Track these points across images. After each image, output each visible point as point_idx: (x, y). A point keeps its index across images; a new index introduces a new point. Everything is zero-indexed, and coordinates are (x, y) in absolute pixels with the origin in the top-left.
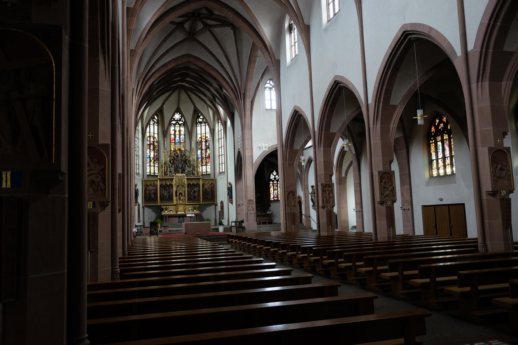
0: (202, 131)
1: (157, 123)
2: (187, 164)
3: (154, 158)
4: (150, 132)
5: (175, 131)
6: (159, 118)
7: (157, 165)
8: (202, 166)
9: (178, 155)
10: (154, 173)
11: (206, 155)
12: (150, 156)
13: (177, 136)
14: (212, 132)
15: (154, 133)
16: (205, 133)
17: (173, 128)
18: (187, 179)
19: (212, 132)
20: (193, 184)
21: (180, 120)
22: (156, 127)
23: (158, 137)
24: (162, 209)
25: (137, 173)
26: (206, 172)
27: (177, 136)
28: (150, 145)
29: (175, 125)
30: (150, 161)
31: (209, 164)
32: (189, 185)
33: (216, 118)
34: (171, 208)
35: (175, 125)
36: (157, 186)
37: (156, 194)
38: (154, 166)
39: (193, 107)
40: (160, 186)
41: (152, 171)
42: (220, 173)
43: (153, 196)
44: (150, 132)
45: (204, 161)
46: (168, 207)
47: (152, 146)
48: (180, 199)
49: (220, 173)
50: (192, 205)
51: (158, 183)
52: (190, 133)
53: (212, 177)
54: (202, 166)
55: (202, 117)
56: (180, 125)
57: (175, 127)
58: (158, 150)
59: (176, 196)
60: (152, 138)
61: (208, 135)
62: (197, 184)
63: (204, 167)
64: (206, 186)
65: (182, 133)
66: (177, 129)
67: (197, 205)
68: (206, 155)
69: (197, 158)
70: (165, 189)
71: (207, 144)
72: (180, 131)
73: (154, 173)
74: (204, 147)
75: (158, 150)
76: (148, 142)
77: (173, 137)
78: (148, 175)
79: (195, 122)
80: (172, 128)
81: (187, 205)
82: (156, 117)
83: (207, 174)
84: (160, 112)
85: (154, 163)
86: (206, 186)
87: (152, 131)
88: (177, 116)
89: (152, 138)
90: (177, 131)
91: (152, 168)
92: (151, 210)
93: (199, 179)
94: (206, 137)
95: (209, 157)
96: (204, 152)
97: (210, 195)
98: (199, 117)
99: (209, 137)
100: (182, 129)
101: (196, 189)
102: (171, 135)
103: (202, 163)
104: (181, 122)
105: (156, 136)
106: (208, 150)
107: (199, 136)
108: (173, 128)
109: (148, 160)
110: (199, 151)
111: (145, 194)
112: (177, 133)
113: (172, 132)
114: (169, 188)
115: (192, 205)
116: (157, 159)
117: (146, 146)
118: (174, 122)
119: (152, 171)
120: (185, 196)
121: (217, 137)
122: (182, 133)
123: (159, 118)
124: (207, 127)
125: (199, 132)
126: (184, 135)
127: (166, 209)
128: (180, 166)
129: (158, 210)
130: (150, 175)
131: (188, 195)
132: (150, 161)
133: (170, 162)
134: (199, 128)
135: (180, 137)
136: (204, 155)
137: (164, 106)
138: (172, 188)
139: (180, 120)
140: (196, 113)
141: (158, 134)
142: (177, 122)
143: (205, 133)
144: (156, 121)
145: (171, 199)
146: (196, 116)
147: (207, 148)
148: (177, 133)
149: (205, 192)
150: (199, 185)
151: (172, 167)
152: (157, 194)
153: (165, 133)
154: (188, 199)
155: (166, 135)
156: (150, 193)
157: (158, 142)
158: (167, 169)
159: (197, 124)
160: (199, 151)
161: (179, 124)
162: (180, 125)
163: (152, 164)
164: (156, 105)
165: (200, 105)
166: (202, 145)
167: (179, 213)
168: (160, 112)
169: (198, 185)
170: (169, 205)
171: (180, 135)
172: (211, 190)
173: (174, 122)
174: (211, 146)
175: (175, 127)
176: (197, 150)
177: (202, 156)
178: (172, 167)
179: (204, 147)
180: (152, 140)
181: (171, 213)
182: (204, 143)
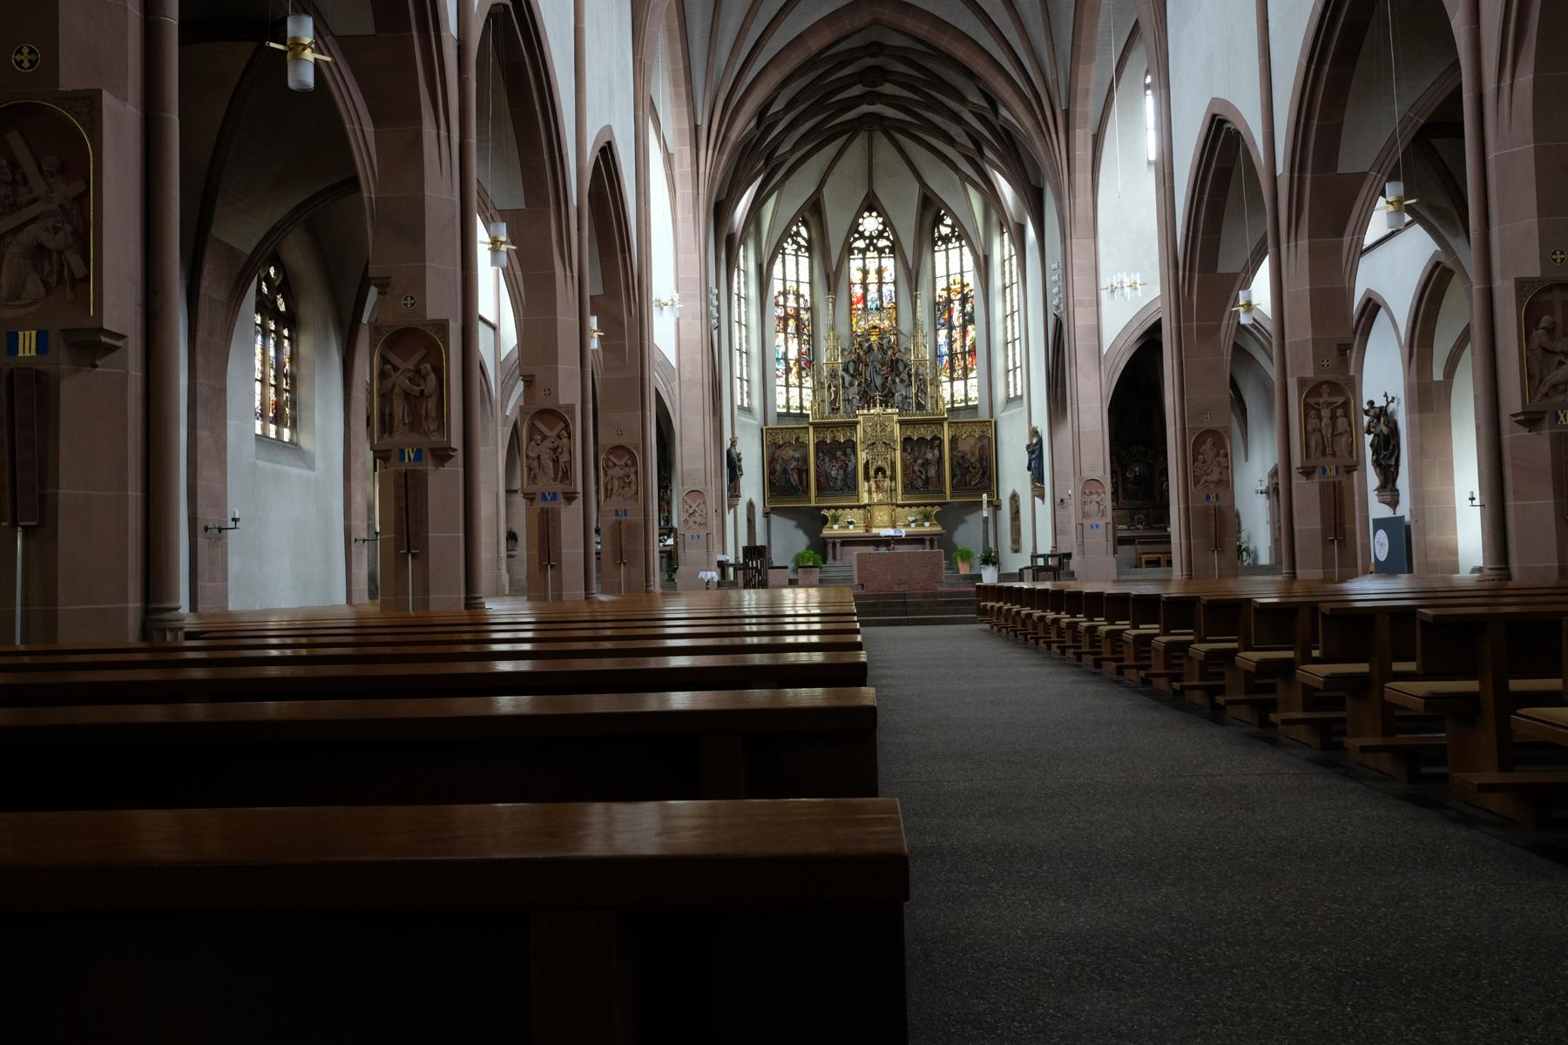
0: (951, 265)
1: (808, 249)
2: (898, 375)
3: (798, 361)
4: (784, 280)
5: (865, 272)
6: (814, 235)
7: (808, 382)
8: (952, 380)
9: (870, 347)
10: (801, 407)
11: (964, 346)
12: (785, 354)
13: (873, 288)
14: (983, 266)
15: (798, 282)
16: (962, 273)
17: (859, 263)
18: (901, 423)
19: (983, 266)
20: (922, 439)
21: (880, 235)
22: (804, 262)
23: (812, 295)
24: (825, 520)
25: (741, 408)
26: (966, 399)
27: (873, 288)
28: (785, 319)
29: (863, 251)
30: (788, 371)
31: (973, 374)
32: (907, 441)
33: (994, 218)
34: (849, 515)
35: (863, 251)
36: (806, 446)
37: (803, 471)
38: (801, 386)
39: (917, 186)
40: (817, 445)
41: (795, 403)
42: (1009, 400)
43: (794, 478)
44: (784, 280)
45: (959, 364)
46: (840, 511)
47: (792, 323)
48: (878, 487)
49: (1009, 400)
50: (918, 505)
51: (811, 439)
52: (912, 276)
53: (984, 415)
54: (952, 380)
55: (948, 221)
56: (881, 251)
57: (864, 259)
58: (811, 336)
59: (867, 478)
60: (791, 298)
61: (970, 278)
62: (935, 438)
63: (959, 385)
64: (964, 446)
65: (889, 276)
66: (872, 265)
67: (933, 505)
68: (964, 346)
69: (937, 356)
70: (834, 457)
71: (968, 308)
72: (880, 272)
73: (801, 407)
74: (957, 319)
75: (811, 336)
76: (780, 312)
77: (858, 291)
78: (780, 415)
79: (927, 237)
80: (855, 264)
81: (903, 506)
82: (803, 231)
83: (967, 408)
84: (813, 212)
85: (800, 377)
86: (964, 446)
87: (791, 275)
88: (871, 224)
89: (791, 298)
90: (872, 272)
91: (794, 392)
92: (791, 524)
93: (940, 422)
94: (963, 286)
95: (973, 352)
96: (956, 334)
97: (978, 471)
98: (939, 220)
99: (972, 286)
100: (889, 263)
101: (929, 456)
102: (851, 284)
103: (952, 370)
104: (882, 243)
105: (805, 290)
106: (970, 328)
107: (941, 284)
108: (859, 263)
109: (782, 367)
110: (943, 333)
111: (772, 472)
112: (872, 278)
113: (856, 276)
114: (845, 454)
115: (918, 505)
116: (808, 362)
117: (772, 322)
118: (861, 244)
119: (795, 403)
120: (893, 478)
121: (996, 282)
122: (889, 276)
123: (814, 235)
124: (966, 250)
125: (940, 270)
126: (895, 283)
127: (836, 520)
128: (878, 381)
129: (813, 521)
130: (788, 414)
131: (904, 474)
132: (788, 371)
133: (846, 370)
134: (940, 257)
135: (880, 291)
136: (957, 346)
137: (826, 191)
138: (855, 452)
139: (880, 235)
140: (931, 209)
141: (811, 283)
142: (871, 243)
143: (962, 273)
144: (803, 243)
145: (850, 487)
146: (929, 219)
147: (968, 319)
148: (872, 278)
149: (960, 464)
150: (941, 442)
151: (851, 384)
152: (805, 472)
153: (832, 278)
154: (904, 487)
155: (836, 285)
156: (785, 471)
157: (811, 309)
158: (836, 393)
159: (934, 243)
160: (943, 333)
161: (876, 248)
162: (881, 251)
163: (793, 379)
164: (800, 189)
165: (940, 181)
166: (950, 311)
167: (875, 531)
168: (813, 212)
169: (936, 442)
170: (844, 508)
171: (880, 283)
172: (981, 459)
173: (861, 244)
174: (979, 315)
175: (864, 259)
176: (936, 330)
177: (950, 348)
178: (851, 384)
179: (957, 319)
180: (791, 303)
181: (851, 531)
182: (956, 306)
